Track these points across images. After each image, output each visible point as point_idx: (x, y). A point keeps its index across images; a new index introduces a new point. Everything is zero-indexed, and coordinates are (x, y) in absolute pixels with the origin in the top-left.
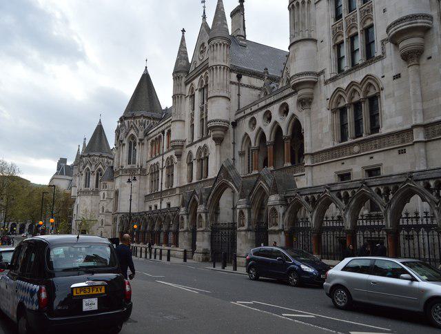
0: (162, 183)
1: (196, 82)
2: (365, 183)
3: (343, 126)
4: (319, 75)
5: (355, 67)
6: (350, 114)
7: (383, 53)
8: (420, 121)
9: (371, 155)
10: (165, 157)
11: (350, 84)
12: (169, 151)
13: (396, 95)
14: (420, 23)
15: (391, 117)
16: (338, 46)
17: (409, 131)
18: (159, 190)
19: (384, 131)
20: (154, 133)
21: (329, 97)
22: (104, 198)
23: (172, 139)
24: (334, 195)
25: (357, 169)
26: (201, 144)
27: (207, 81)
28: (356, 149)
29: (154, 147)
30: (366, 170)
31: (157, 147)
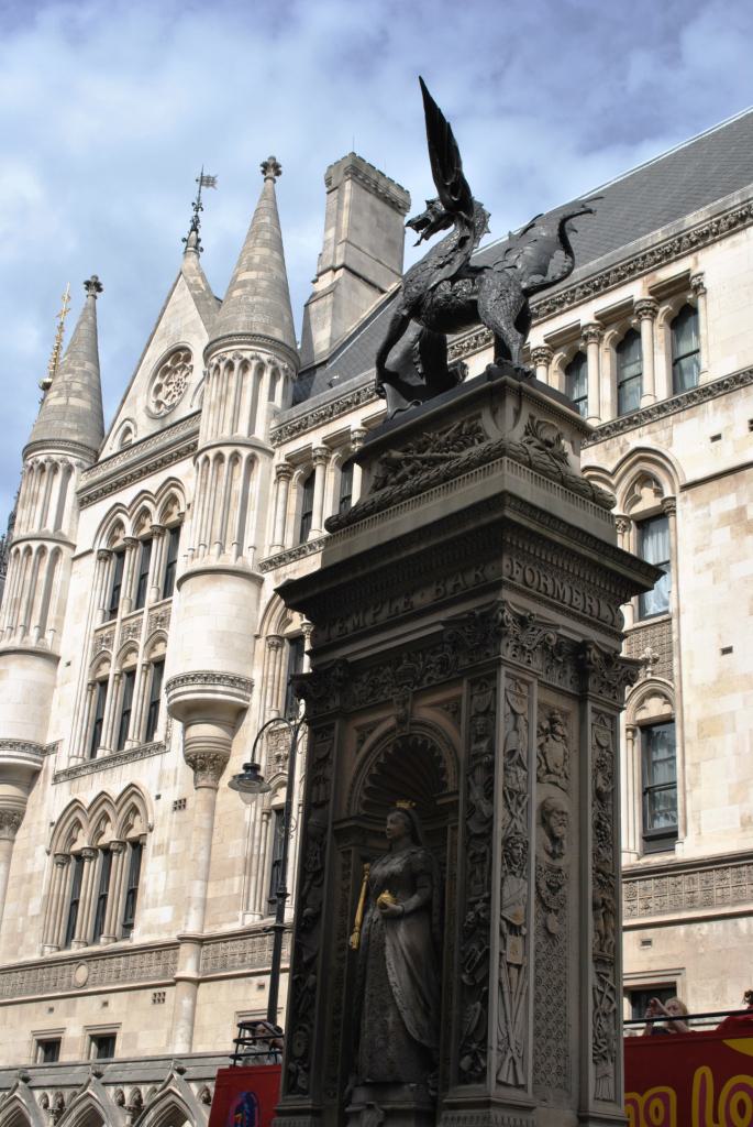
4: (44, 751)
5: (119, 757)
6: (92, 870)
7: (167, 739)
8: (192, 929)
9: (104, 997)
11: (70, 805)
14: (221, 693)
15: (155, 906)
17: (174, 946)
19: (138, 938)
21: (55, 820)
25: (74, 1025)
28: (82, 973)
30: (93, 1038)
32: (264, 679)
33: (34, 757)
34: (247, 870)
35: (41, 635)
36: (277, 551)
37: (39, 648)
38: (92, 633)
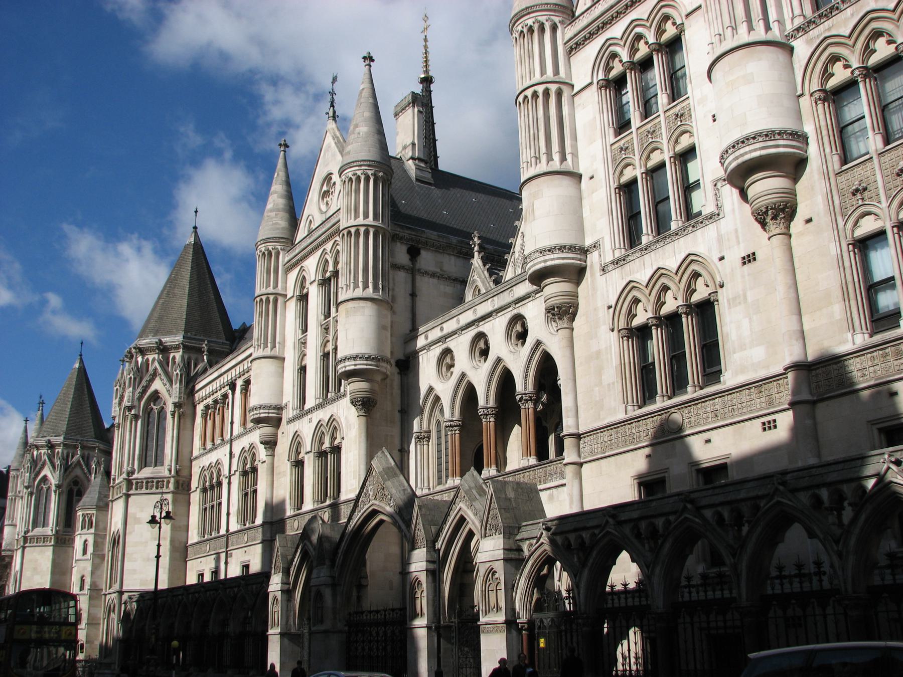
0: (228, 514)
1: (311, 264)
2: (692, 502)
3: (646, 373)
9: (706, 436)
10: (237, 448)
12: (246, 432)
13: (749, 299)
14: (782, 147)
15: (743, 347)
16: (628, 190)
18: (223, 531)
19: (729, 379)
20: (209, 389)
22: (85, 552)
23: (253, 401)
24: (627, 530)
26: (323, 415)
27: (336, 263)
29: (209, 423)
31: (218, 418)
32: (819, 131)
33: (579, 256)
34: (845, 296)
35: (563, 159)
36: (798, 21)
37: (563, 168)
38: (608, 148)
